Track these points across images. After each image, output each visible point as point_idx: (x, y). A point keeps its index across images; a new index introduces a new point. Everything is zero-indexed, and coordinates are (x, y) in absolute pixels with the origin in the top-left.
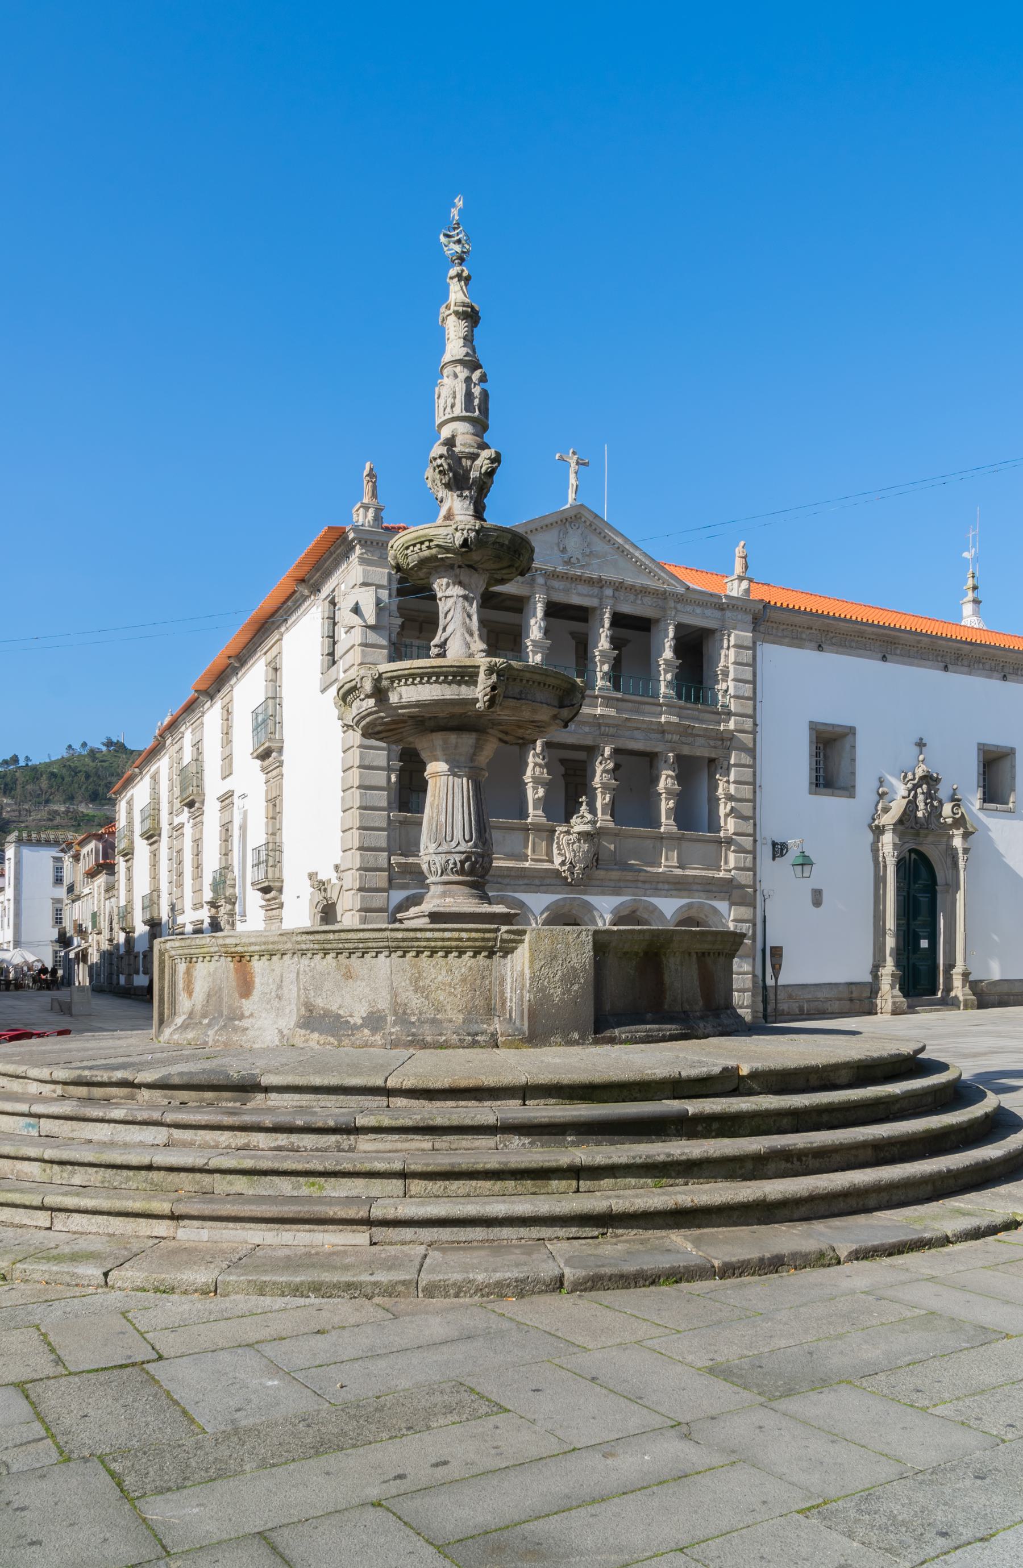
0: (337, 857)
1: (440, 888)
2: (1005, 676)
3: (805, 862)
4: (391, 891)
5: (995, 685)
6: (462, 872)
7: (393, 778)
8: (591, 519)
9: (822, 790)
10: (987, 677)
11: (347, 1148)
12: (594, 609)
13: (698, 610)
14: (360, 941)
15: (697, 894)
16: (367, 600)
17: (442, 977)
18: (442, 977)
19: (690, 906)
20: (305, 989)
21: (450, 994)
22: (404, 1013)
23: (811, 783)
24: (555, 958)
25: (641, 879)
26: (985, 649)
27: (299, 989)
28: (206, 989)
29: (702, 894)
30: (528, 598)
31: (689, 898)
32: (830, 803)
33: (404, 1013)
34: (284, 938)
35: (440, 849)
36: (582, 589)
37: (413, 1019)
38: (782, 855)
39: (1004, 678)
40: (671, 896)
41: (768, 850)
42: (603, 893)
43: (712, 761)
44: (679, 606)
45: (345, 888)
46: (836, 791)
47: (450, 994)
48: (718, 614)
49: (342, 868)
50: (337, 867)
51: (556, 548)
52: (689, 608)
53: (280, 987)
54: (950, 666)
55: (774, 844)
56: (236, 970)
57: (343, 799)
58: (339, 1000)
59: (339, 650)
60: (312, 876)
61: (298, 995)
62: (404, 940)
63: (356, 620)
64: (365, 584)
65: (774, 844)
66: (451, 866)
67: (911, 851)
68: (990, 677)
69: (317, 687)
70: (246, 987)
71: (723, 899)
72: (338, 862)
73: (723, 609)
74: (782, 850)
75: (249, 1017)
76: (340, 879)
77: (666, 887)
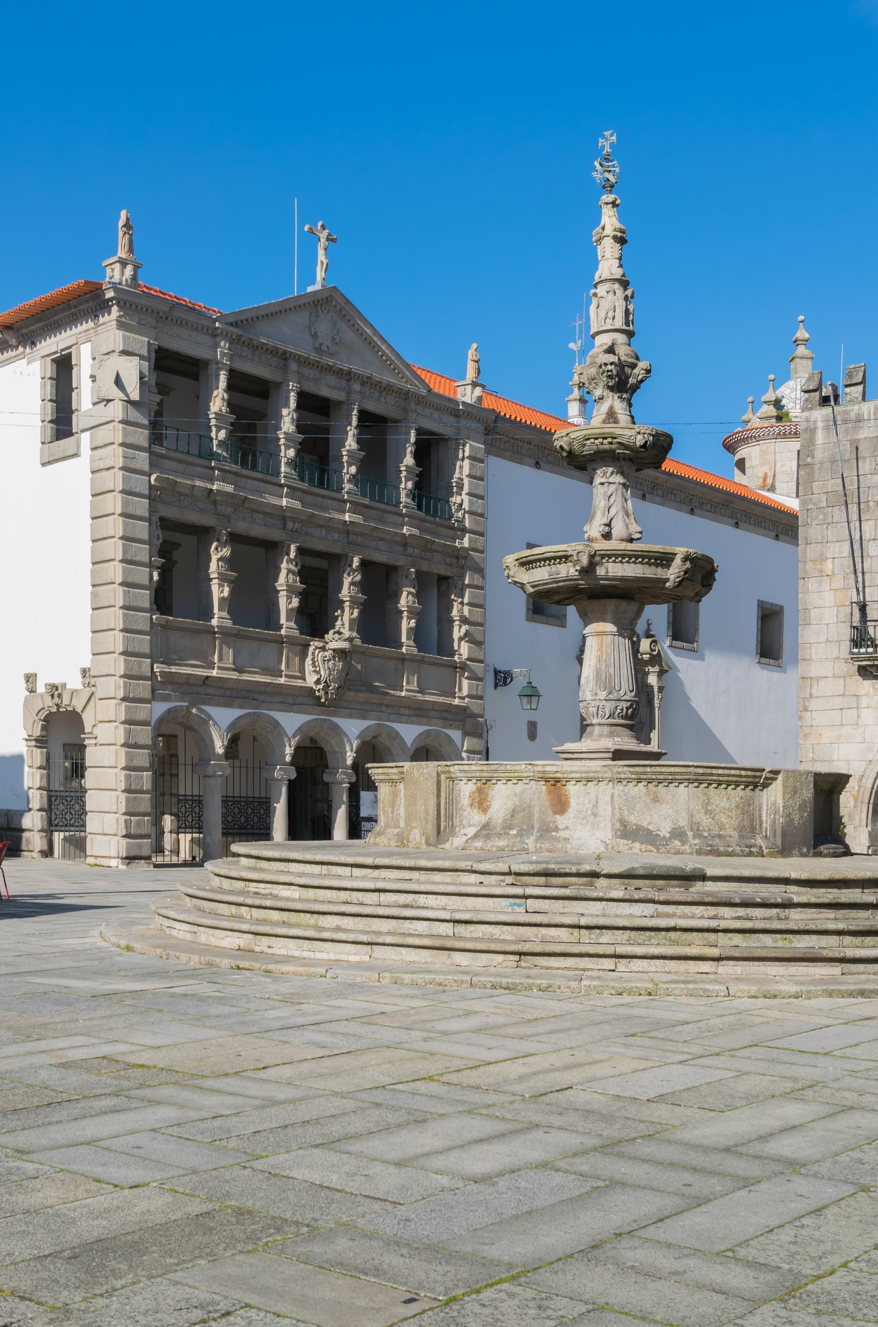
1: (606, 729)
2: (692, 510)
3: (531, 694)
4: (153, 703)
5: (684, 517)
6: (626, 717)
7: (156, 577)
8: (342, 303)
9: (538, 617)
10: (677, 510)
11: (783, 917)
12: (339, 403)
13: (436, 415)
14: (671, 773)
15: (434, 721)
16: (132, 371)
17: (724, 804)
18: (724, 804)
19: (427, 733)
20: (620, 809)
21: (729, 816)
22: (698, 830)
23: (528, 609)
24: (795, 792)
25: (386, 702)
26: (678, 480)
27: (613, 809)
28: (510, 805)
29: (439, 722)
30: (278, 385)
31: (427, 725)
33: (698, 830)
34: (606, 769)
35: (611, 697)
36: (331, 379)
37: (706, 834)
38: (505, 684)
39: (692, 512)
40: (412, 723)
42: (351, 716)
43: (442, 579)
44: (419, 409)
45: (99, 694)
46: (550, 619)
47: (729, 816)
48: (453, 420)
49: (93, 673)
50: (85, 672)
51: (307, 332)
52: (427, 412)
53: (595, 806)
54: (647, 495)
55: (496, 672)
56: (549, 792)
58: (649, 818)
59: (77, 422)
61: (613, 814)
62: (703, 774)
63: (116, 393)
64: (125, 353)
65: (496, 672)
66: (618, 711)
68: (679, 510)
70: (560, 805)
71: (457, 728)
73: (457, 416)
74: (505, 678)
75: (564, 829)
77: (407, 712)
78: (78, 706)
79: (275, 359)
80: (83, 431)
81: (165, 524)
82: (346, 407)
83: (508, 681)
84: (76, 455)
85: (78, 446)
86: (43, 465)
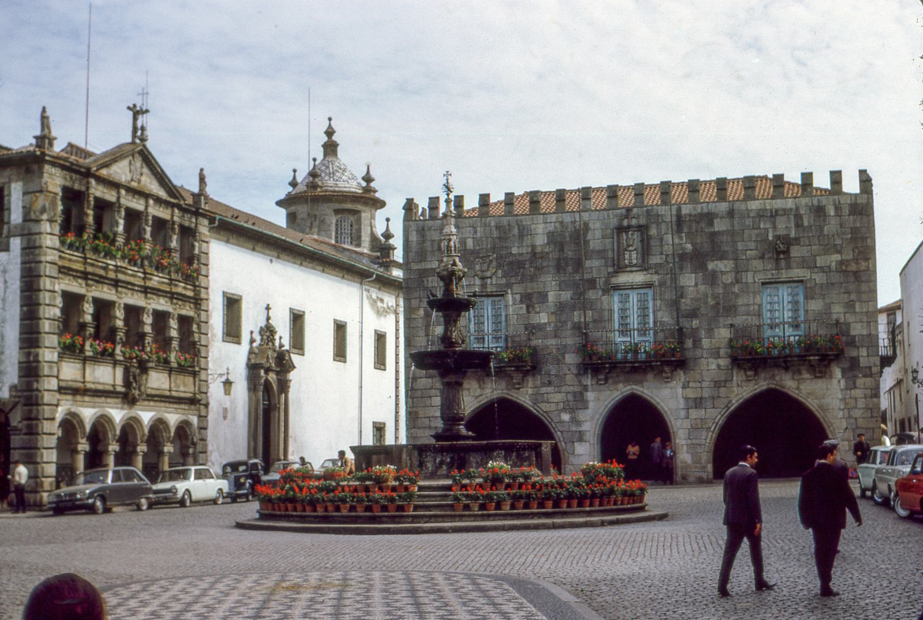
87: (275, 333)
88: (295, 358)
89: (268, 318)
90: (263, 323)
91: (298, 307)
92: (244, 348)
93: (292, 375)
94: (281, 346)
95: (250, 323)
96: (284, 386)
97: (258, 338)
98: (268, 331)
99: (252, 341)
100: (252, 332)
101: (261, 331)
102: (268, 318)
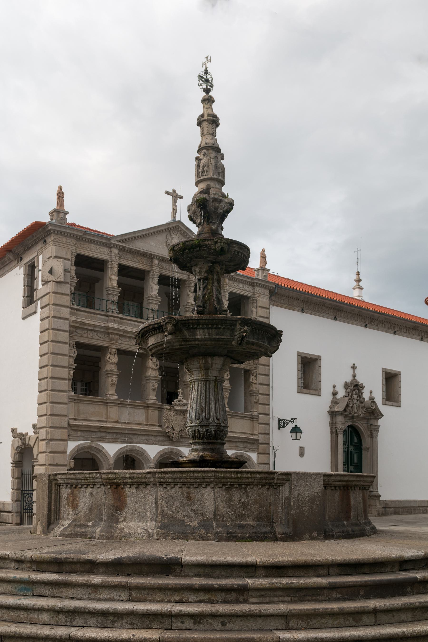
0: (35, 420)
2: (395, 332)
8: (184, 229)
10: (386, 332)
13: (241, 285)
16: (59, 266)
26: (385, 317)
32: (308, 399)
38: (284, 427)
41: (274, 424)
44: (231, 282)
45: (40, 438)
46: (312, 392)
48: (250, 289)
49: (38, 426)
51: (165, 245)
54: (368, 325)
55: (279, 420)
57: (39, 384)
60: (13, 430)
64: (56, 257)
65: (279, 420)
67: (349, 427)
68: (388, 332)
69: (20, 316)
71: (253, 452)
72: (36, 422)
73: (253, 286)
74: (284, 423)
76: (35, 433)
78: (32, 444)
79: (146, 258)
80: (39, 299)
81: (79, 345)
82: (188, 282)
83: (285, 425)
84: (35, 313)
85: (36, 307)
86: (24, 319)
87: (363, 387)
88: (383, 408)
89: (354, 376)
90: (349, 379)
91: (393, 367)
92: (324, 401)
93: (381, 422)
94: (372, 399)
95: (333, 378)
96: (373, 433)
97: (341, 393)
98: (354, 388)
99: (335, 394)
100: (334, 387)
101: (346, 385)
102: (354, 376)
